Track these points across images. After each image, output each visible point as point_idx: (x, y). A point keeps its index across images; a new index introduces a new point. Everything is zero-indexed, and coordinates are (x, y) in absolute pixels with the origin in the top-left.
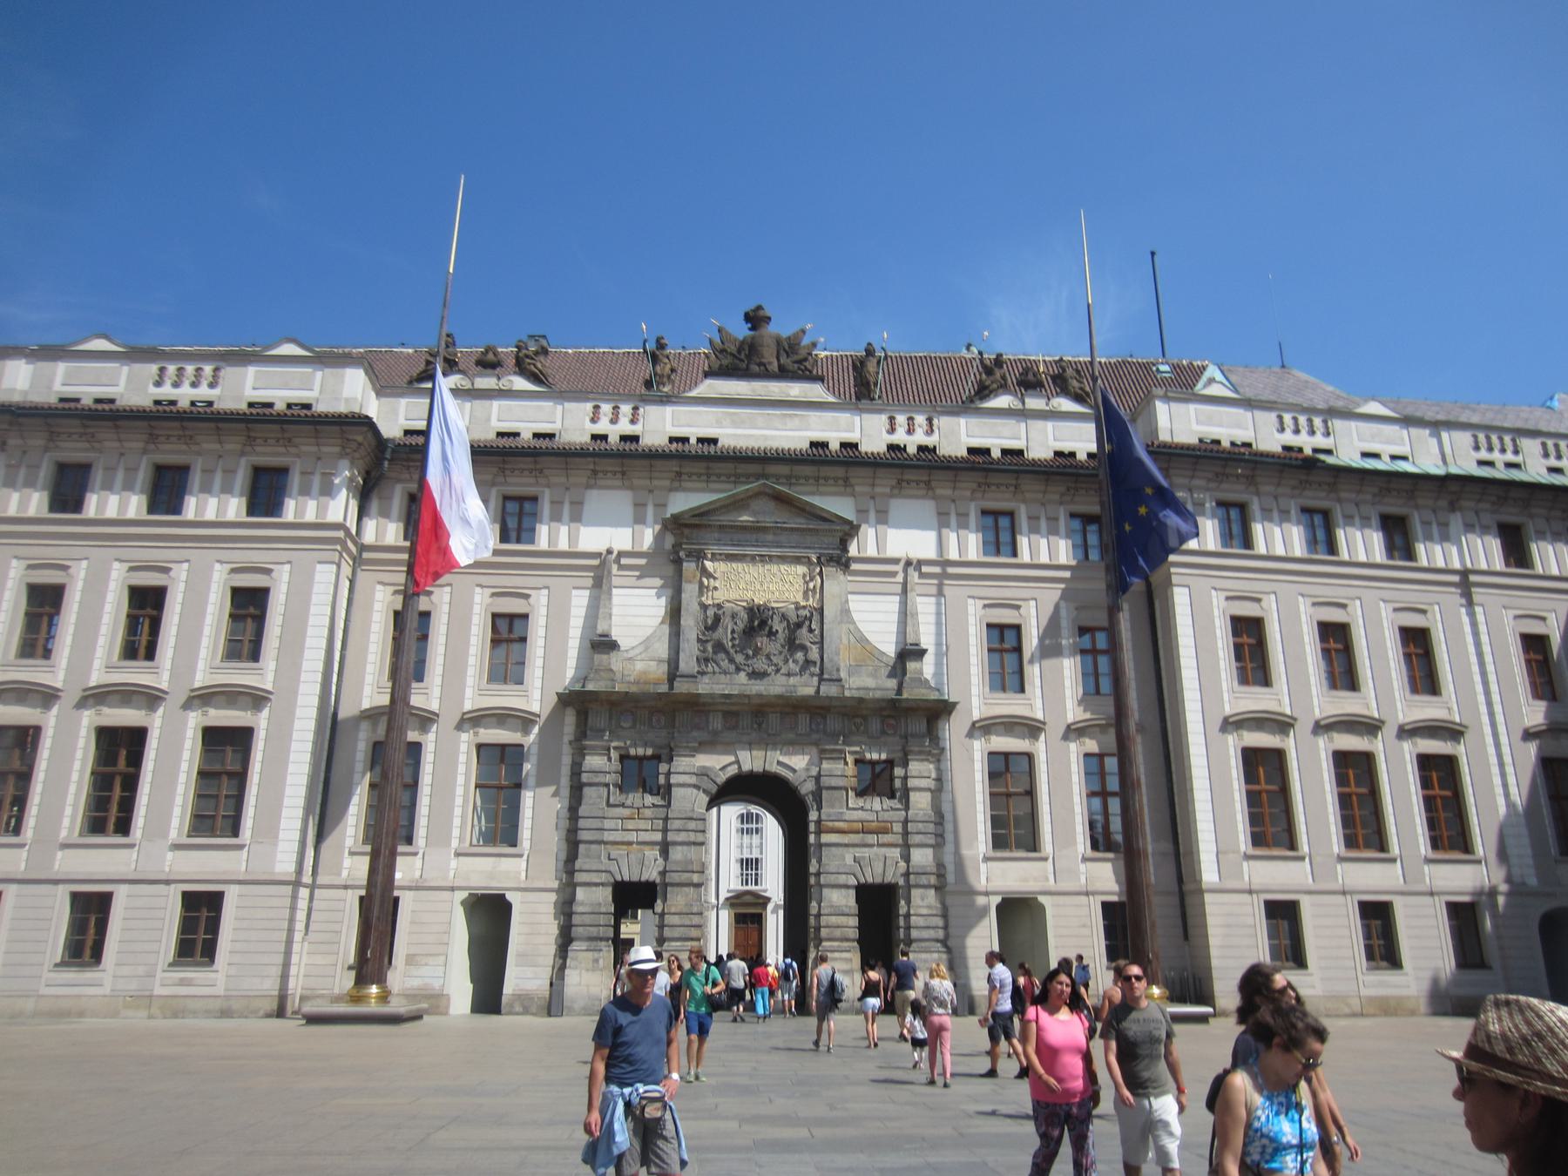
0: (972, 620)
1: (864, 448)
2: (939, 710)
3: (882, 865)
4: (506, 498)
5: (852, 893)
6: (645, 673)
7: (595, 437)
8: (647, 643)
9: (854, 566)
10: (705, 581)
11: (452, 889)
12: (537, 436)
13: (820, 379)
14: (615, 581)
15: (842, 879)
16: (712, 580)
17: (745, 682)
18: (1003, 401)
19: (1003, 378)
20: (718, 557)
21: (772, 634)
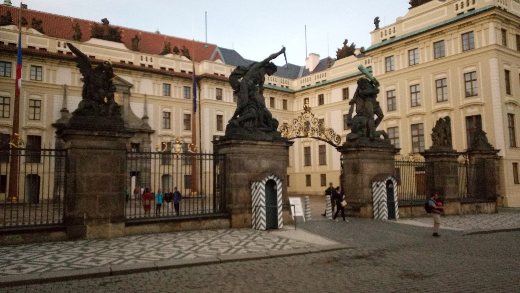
2: (151, 132)
9: (132, 95)
13: (124, 43)
14: (67, 94)
18: (170, 55)
19: (170, 49)
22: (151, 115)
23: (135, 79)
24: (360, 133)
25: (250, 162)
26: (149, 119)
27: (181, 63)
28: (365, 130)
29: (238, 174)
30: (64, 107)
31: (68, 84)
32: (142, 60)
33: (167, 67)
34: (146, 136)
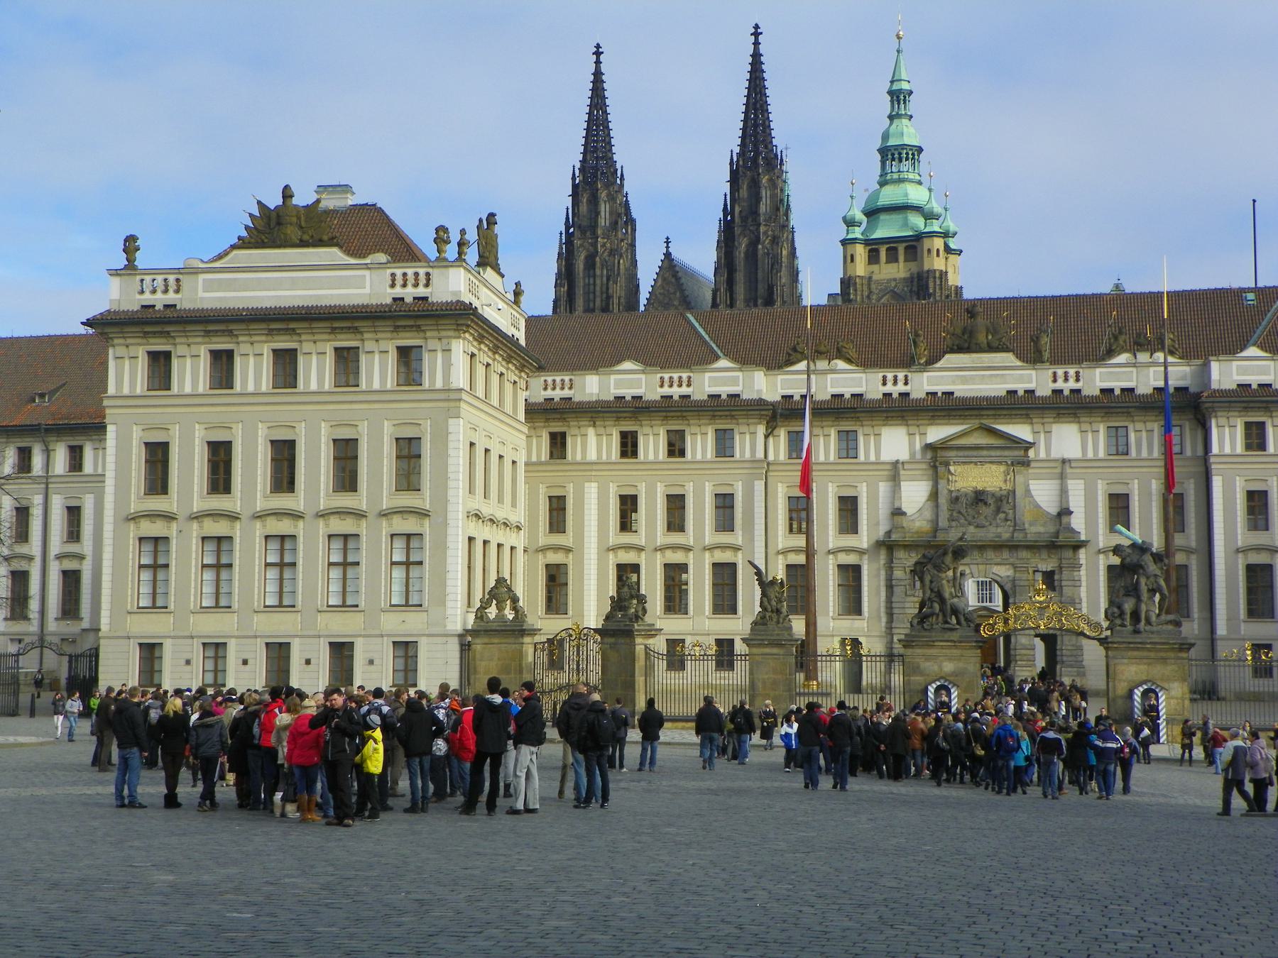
0: (1100, 492)
1: (1038, 394)
2: (1077, 546)
9: (1033, 465)
10: (950, 477)
11: (833, 636)
13: (1012, 351)
14: (902, 478)
18: (1123, 358)
21: (986, 503)
22: (1077, 502)
23: (1038, 427)
25: (928, 664)
26: (1073, 515)
27: (1152, 369)
28: (1128, 617)
29: (912, 678)
30: (896, 505)
32: (1055, 381)
33: (1117, 385)
34: (1068, 553)
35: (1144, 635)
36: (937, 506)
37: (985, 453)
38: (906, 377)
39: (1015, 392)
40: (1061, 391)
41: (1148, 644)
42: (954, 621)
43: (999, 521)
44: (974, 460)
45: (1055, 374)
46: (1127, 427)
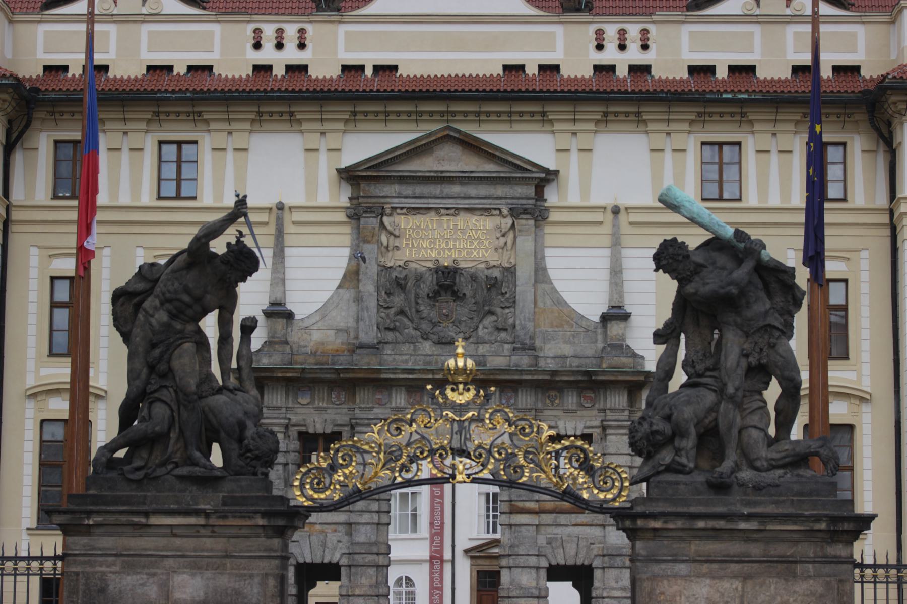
1: (565, 72)
3: (575, 546)
4: (161, 143)
5: (543, 573)
6: (323, 344)
7: (257, 69)
8: (323, 311)
9: (554, 216)
10: (384, 238)
12: (191, 68)
14: (288, 240)
15: (533, 561)
16: (392, 237)
17: (430, 353)
20: (398, 211)
21: (457, 296)
23: (565, 140)
24: (666, 456)
25: (130, 580)
28: (689, 443)
30: (278, 296)
31: (288, 202)
35: (736, 496)
36: (359, 299)
37: (456, 189)
38: (302, 31)
39: (521, 68)
40: (611, 69)
41: (749, 517)
42: (216, 457)
43: (481, 332)
44: (433, 203)
45: (600, 33)
46: (739, 144)
